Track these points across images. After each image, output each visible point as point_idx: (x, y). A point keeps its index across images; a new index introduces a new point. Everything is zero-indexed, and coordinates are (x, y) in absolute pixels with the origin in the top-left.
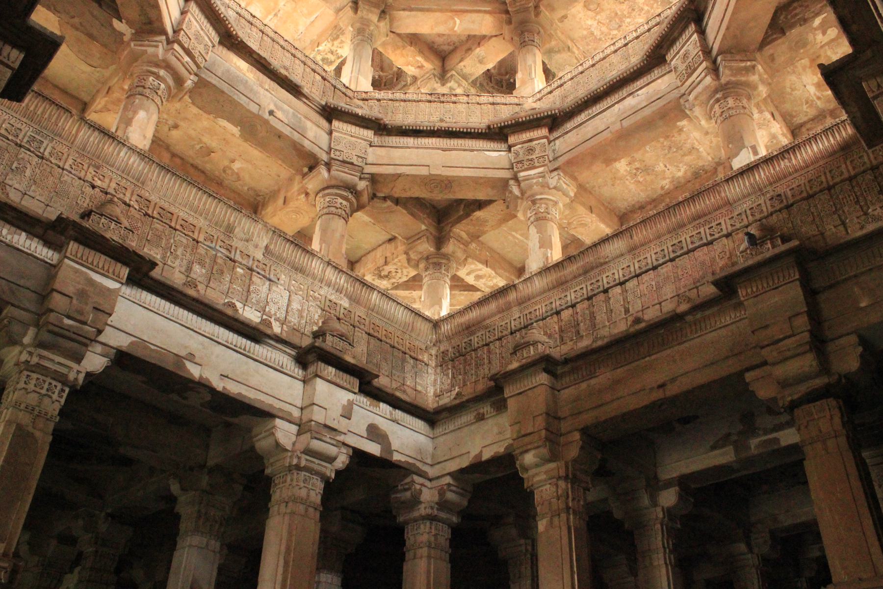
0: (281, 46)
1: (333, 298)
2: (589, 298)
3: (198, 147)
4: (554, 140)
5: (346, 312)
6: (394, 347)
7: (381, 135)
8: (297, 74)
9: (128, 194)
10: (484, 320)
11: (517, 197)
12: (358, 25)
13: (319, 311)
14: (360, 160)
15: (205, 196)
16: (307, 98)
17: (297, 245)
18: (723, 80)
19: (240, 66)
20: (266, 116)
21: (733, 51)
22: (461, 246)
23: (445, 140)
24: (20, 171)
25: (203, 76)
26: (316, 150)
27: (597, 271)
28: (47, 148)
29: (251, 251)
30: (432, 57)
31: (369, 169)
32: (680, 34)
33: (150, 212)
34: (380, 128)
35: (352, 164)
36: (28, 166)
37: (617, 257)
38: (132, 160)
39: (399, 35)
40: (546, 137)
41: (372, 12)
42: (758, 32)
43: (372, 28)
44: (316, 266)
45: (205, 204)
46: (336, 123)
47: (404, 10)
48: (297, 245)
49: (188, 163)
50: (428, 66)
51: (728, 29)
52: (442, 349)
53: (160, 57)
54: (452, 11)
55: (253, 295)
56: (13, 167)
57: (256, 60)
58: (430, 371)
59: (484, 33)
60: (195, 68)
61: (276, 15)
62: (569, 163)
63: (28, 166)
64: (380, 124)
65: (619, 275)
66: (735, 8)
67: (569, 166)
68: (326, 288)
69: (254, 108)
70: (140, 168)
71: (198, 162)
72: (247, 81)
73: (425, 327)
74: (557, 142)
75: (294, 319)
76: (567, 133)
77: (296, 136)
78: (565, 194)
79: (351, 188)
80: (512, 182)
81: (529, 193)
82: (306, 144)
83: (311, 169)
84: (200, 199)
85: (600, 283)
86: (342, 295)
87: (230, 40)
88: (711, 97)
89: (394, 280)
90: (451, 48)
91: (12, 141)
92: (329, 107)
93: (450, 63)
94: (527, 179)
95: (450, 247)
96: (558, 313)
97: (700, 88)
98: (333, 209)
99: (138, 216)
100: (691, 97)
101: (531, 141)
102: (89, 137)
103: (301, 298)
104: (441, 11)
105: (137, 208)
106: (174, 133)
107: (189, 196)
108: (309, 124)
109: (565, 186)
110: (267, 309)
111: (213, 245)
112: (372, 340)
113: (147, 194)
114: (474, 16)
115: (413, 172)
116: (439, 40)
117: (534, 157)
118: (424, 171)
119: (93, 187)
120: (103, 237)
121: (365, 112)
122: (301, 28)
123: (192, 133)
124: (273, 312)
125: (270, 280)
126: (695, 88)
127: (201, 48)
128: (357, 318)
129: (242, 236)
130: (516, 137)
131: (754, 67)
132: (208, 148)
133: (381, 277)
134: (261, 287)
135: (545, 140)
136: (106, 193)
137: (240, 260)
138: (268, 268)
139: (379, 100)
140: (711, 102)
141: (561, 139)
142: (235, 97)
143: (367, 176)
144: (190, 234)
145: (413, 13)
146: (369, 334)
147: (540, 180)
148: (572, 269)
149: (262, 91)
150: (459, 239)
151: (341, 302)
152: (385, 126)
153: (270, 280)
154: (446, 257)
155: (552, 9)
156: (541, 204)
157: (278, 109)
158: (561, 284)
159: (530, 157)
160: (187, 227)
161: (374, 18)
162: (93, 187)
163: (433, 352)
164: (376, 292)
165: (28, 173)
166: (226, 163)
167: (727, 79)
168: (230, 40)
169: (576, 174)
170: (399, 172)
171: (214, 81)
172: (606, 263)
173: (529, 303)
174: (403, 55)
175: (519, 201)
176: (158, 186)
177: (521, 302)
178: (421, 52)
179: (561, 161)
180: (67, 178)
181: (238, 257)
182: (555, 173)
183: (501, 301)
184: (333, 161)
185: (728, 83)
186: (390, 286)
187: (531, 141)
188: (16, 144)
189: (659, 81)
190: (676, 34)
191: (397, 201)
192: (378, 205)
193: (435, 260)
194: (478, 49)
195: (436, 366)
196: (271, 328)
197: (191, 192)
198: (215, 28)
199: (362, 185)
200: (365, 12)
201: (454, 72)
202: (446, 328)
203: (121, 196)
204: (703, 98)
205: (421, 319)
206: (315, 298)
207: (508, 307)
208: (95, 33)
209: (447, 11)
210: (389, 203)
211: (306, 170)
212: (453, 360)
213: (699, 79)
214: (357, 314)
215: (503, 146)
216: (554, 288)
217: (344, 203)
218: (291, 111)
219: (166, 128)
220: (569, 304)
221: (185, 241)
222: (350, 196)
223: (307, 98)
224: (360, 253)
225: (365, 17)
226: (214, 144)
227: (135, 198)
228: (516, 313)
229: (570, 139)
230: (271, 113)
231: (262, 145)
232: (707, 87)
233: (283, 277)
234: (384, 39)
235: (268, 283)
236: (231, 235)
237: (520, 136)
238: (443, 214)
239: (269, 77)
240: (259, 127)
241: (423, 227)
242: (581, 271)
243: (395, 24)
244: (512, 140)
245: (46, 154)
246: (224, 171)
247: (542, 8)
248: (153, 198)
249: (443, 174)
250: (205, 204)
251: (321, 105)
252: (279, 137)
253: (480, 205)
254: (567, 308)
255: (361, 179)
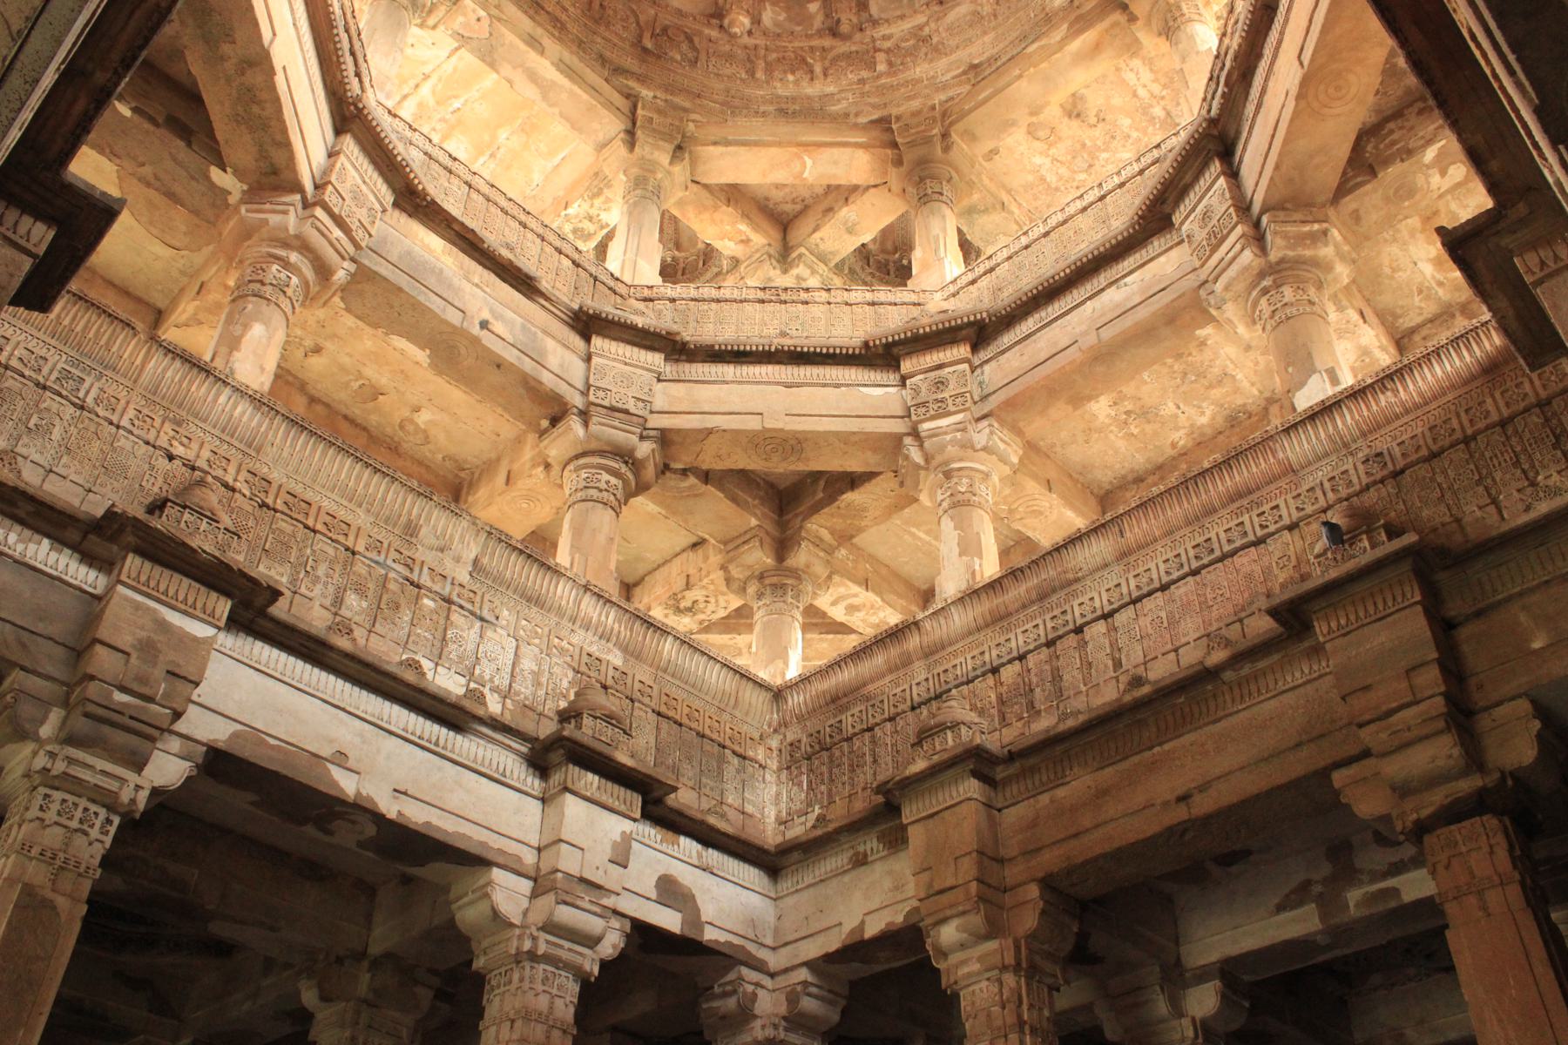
0: (502, 210)
1: (594, 649)
2: (1050, 644)
3: (356, 385)
4: (981, 365)
5: (617, 675)
6: (703, 736)
7: (677, 361)
8: (529, 258)
9: (232, 470)
10: (865, 685)
11: (918, 467)
12: (635, 171)
13: (571, 674)
14: (641, 404)
15: (367, 472)
16: (547, 299)
17: (530, 556)
18: (1274, 256)
19: (429, 244)
20: (476, 330)
21: (1288, 205)
22: (822, 554)
23: (789, 368)
24: (43, 431)
25: (366, 262)
26: (563, 389)
27: (1062, 594)
28: (91, 390)
29: (449, 567)
30: (766, 225)
31: (656, 422)
32: (1196, 179)
33: (269, 501)
34: (676, 349)
35: (627, 412)
36: (57, 421)
37: (1098, 569)
38: (239, 409)
39: (706, 186)
40: (967, 361)
41: (658, 148)
42: (1328, 173)
43: (659, 176)
44: (563, 592)
45: (367, 485)
46: (597, 342)
47: (715, 143)
48: (530, 556)
49: (337, 413)
50: (758, 239)
51: (1277, 167)
52: (790, 737)
53: (292, 232)
54: (799, 145)
55: (452, 646)
56: (31, 425)
57: (458, 234)
58: (768, 777)
59: (855, 182)
60: (351, 249)
61: (492, 155)
62: (1010, 404)
63: (57, 421)
64: (675, 342)
65: (1102, 602)
66: (1289, 132)
67: (1008, 410)
68: (582, 632)
69: (453, 317)
70: (254, 424)
71: (356, 411)
72: (441, 271)
73: (758, 699)
74: (987, 368)
75: (524, 689)
76: (1003, 352)
77: (528, 365)
78: (1003, 460)
79: (624, 455)
80: (908, 440)
81: (939, 459)
82: (547, 379)
83: (555, 421)
84: (359, 478)
85: (1069, 617)
86: (610, 645)
87: (413, 200)
88: (1253, 286)
89: (701, 617)
90: (798, 207)
91: (30, 378)
92: (587, 313)
93: (795, 235)
94: (934, 434)
95: (801, 557)
96: (995, 671)
97: (1232, 272)
98: (594, 493)
99: (250, 509)
100: (1219, 286)
101: (940, 367)
102: (165, 370)
103: (537, 650)
104: (779, 144)
105: (248, 493)
106: (316, 362)
107: (339, 471)
108: (550, 344)
109: (1002, 446)
110: (477, 672)
111: (381, 559)
112: (665, 725)
113: (266, 470)
114: (836, 151)
115: (734, 426)
116: (777, 195)
117: (946, 395)
118: (753, 424)
119: (171, 458)
120: (184, 544)
121: (648, 321)
122: (537, 177)
123: (346, 360)
124: (487, 677)
125: (482, 619)
126: (1224, 270)
127: (362, 214)
128: (637, 686)
129: (433, 541)
130: (914, 360)
131: (1325, 233)
132: (373, 387)
133: (679, 611)
134: (465, 631)
135: (966, 366)
136: (193, 468)
137: (429, 584)
138: (478, 599)
139: (673, 300)
140: (1254, 293)
141: (993, 364)
142: (421, 298)
143: (652, 433)
144: (341, 538)
145: (730, 149)
146: (659, 714)
147: (959, 435)
148: (1017, 592)
149: (468, 287)
150: (818, 543)
151: (610, 657)
152: (684, 344)
153: (482, 619)
154: (795, 574)
155: (972, 137)
156: (960, 477)
157: (496, 318)
158: (999, 619)
159: (940, 396)
160: (336, 528)
161: (664, 158)
162: (171, 458)
163: (774, 743)
164: (670, 639)
165: (57, 434)
166: (406, 413)
167: (1280, 255)
168: (413, 200)
169: (1021, 424)
170: (709, 425)
171: (384, 270)
172: (1077, 580)
173: (944, 653)
174: (713, 221)
175: (922, 473)
176: (285, 454)
177: (931, 652)
178: (746, 216)
179: (993, 402)
180: (124, 442)
181: (425, 580)
182: (985, 423)
183: (894, 652)
184: (592, 408)
185: (1282, 261)
186: (695, 627)
187: (940, 367)
188: (38, 384)
189: (1162, 259)
190: (1188, 178)
191: (706, 477)
192: (672, 483)
193: (775, 580)
194: (845, 210)
195: (780, 769)
196: (485, 704)
197: (342, 466)
198: (387, 181)
199: (644, 449)
200: (647, 149)
201: (802, 250)
202: (796, 700)
203: (219, 473)
204: (1240, 287)
205: (750, 685)
206: (562, 651)
207: (906, 661)
208: (177, 189)
209: (790, 144)
210: (692, 480)
211: (545, 423)
212: (809, 759)
214: (638, 677)
215: (893, 377)
216: (987, 626)
217: (613, 480)
218: (519, 320)
219: (300, 354)
220: (1015, 654)
221: (331, 551)
222: (624, 469)
223: (547, 299)
224: (642, 569)
225: (648, 157)
226: (383, 380)
227: (243, 475)
228: (919, 671)
229: (1008, 362)
230: (484, 325)
231: (467, 380)
232: (1246, 269)
233: (506, 613)
234: (680, 194)
235: (478, 624)
236: (414, 540)
237: (922, 360)
238: (789, 497)
239: (480, 264)
240: (463, 351)
241: (754, 522)
242: (1034, 596)
243: (701, 168)
244: (907, 366)
245: (90, 400)
246: (401, 427)
247: (955, 137)
248: (276, 476)
249: (787, 428)
250: (367, 485)
251: (571, 310)
252: (498, 366)
253: (853, 481)
254: (1010, 662)
255: (642, 438)
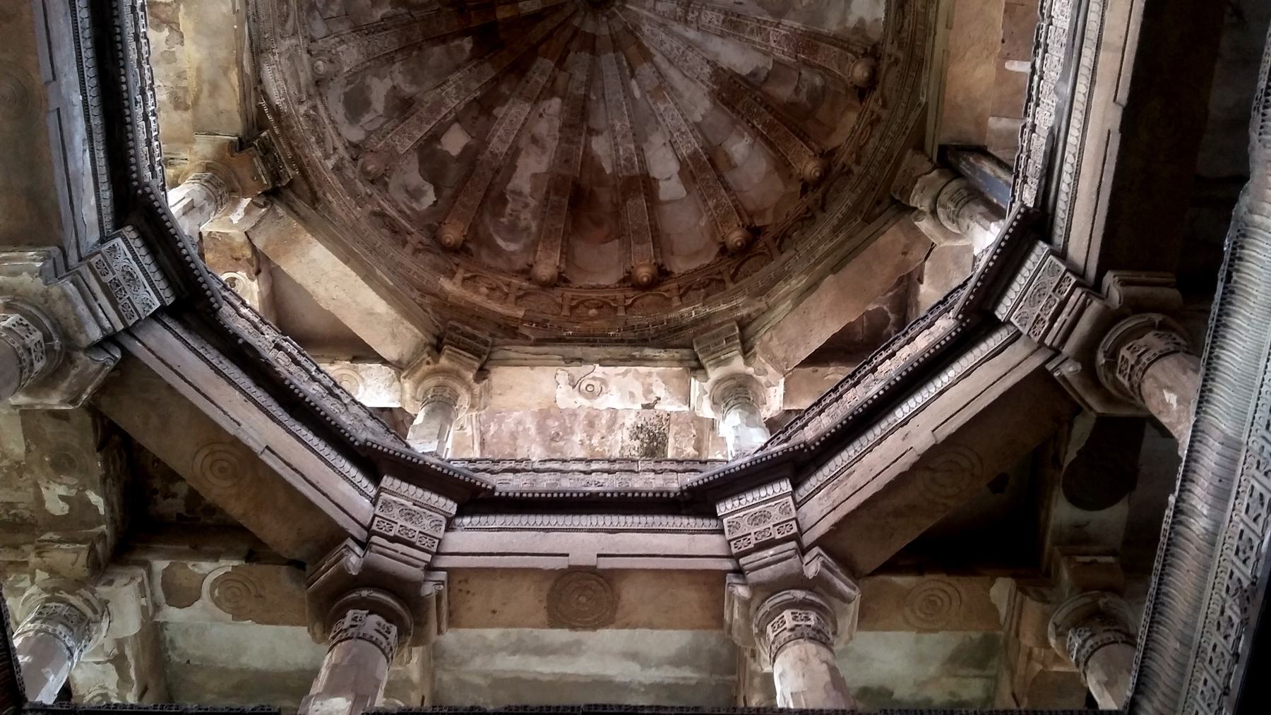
18: (82, 357)
88: (56, 323)
97: (82, 309)
140: (47, 323)
189: (93, 201)
190: (163, 257)
204: (60, 308)
213: (102, 315)
232: (81, 325)
